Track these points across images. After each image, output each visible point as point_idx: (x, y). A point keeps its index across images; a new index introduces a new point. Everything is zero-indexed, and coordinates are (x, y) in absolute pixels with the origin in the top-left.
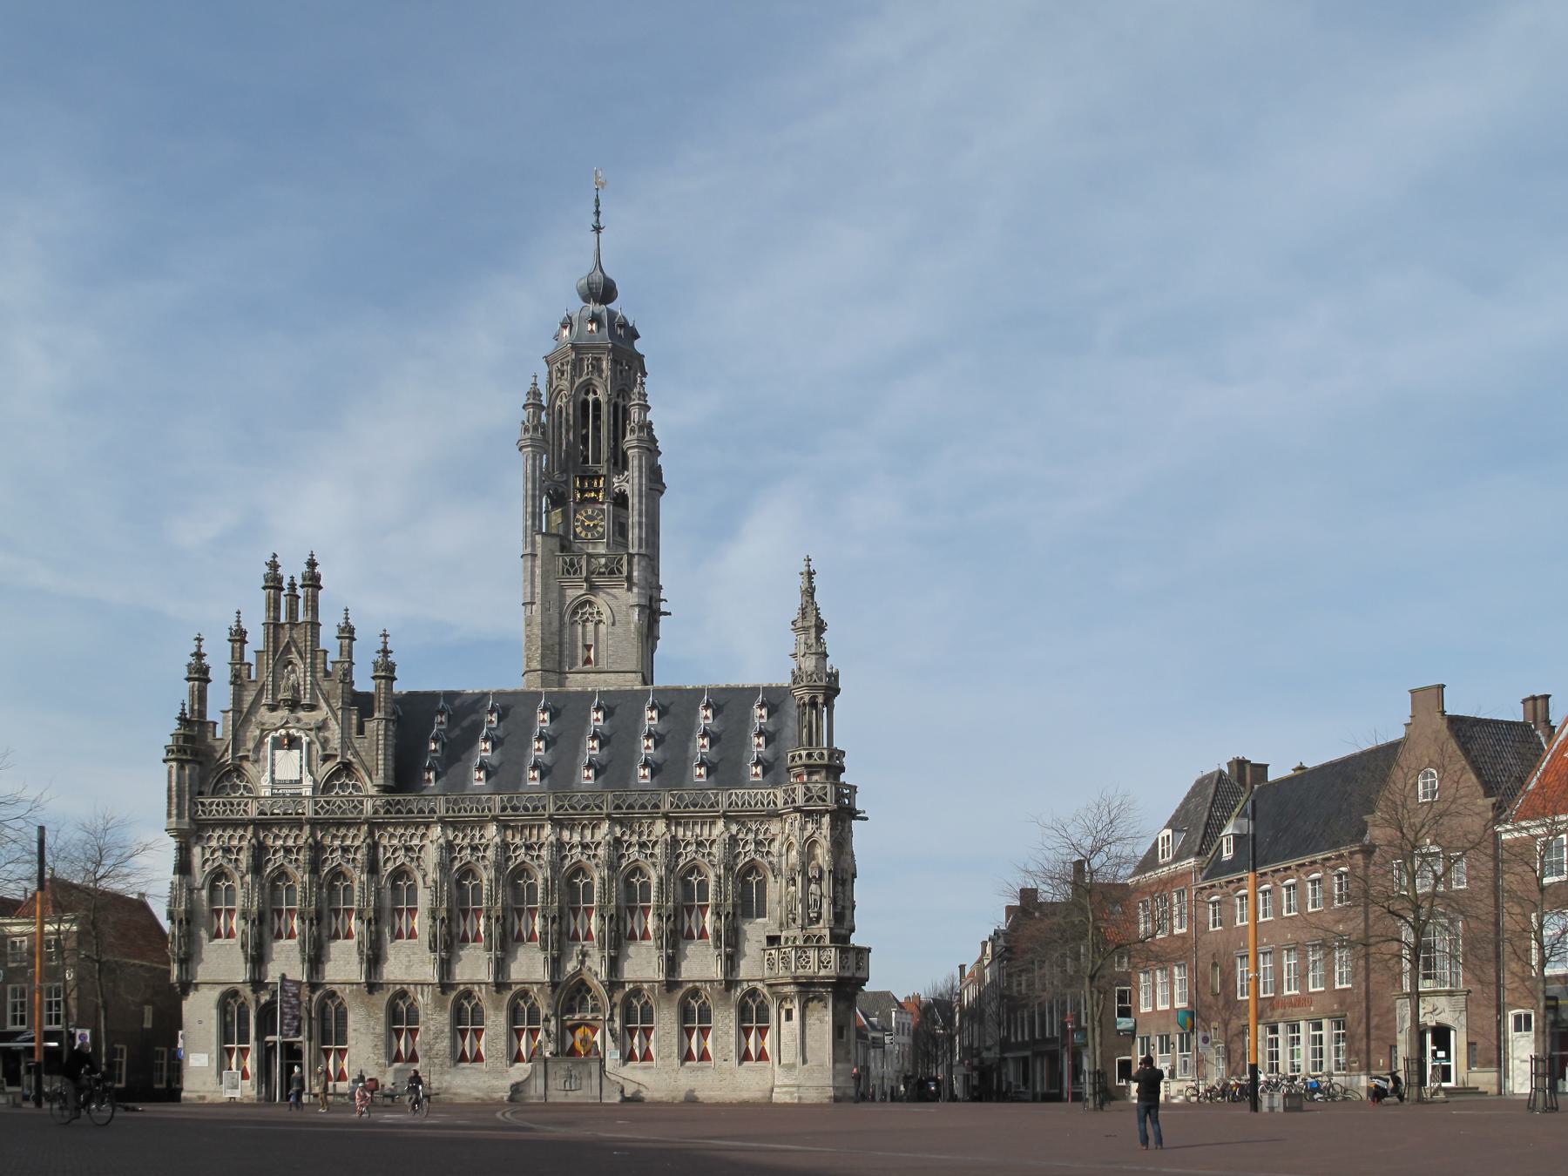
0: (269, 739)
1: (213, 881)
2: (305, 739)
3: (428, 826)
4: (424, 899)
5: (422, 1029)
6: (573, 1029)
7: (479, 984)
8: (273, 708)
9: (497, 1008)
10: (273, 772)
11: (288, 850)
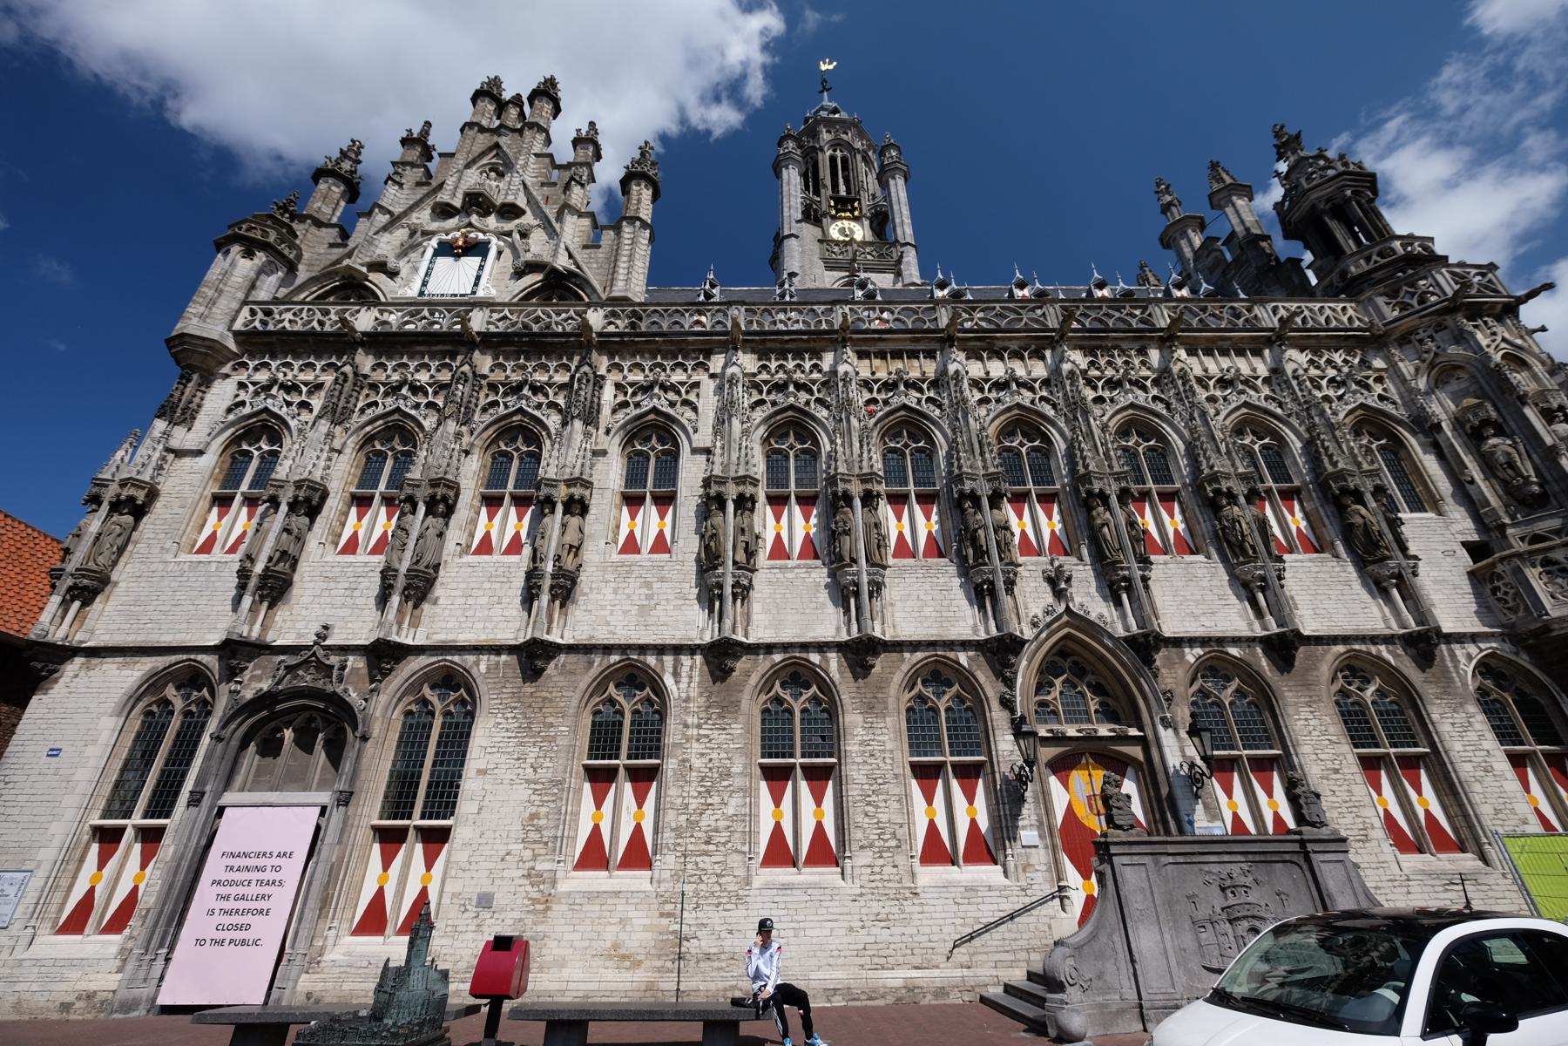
0: (434, 242)
1: (235, 441)
2: (495, 244)
3: (708, 354)
4: (691, 473)
5: (670, 765)
6: (1061, 767)
7: (822, 647)
8: (444, 211)
9: (872, 708)
10: (424, 284)
11: (416, 389)
